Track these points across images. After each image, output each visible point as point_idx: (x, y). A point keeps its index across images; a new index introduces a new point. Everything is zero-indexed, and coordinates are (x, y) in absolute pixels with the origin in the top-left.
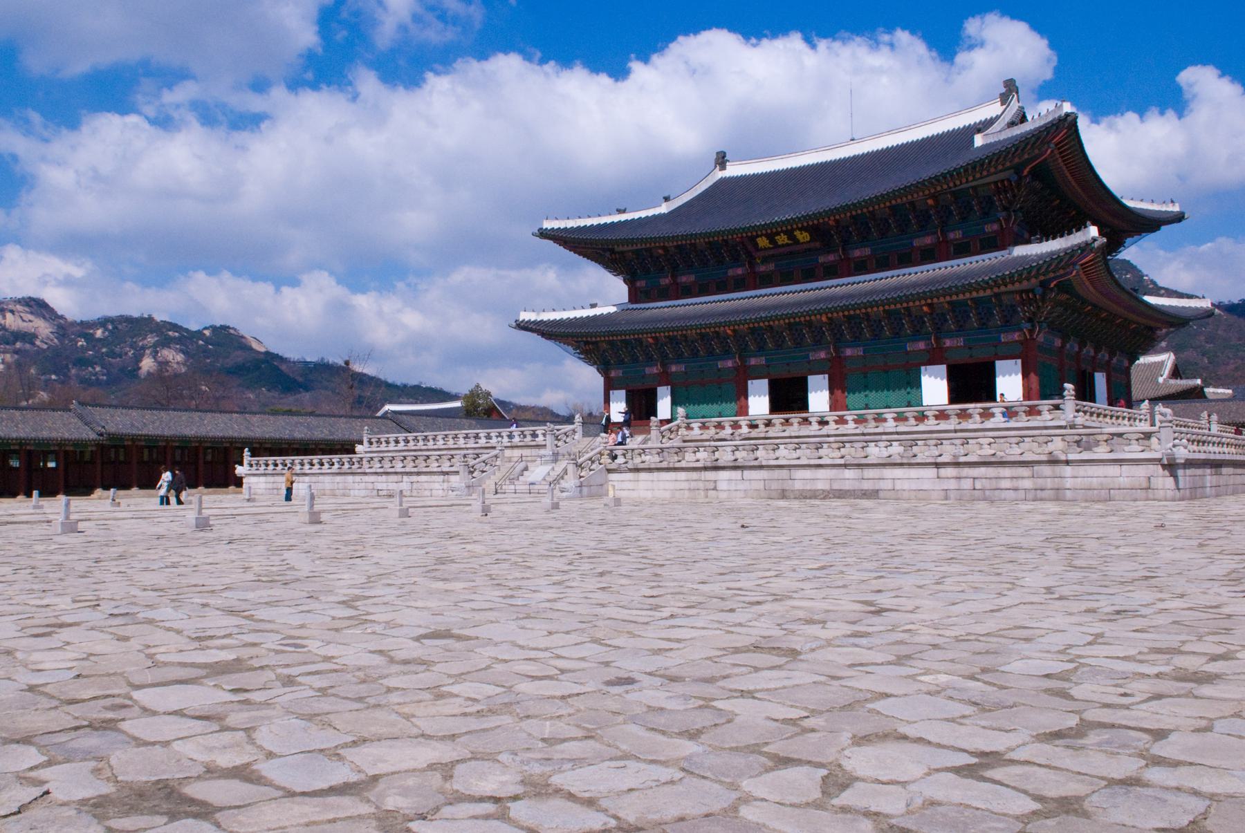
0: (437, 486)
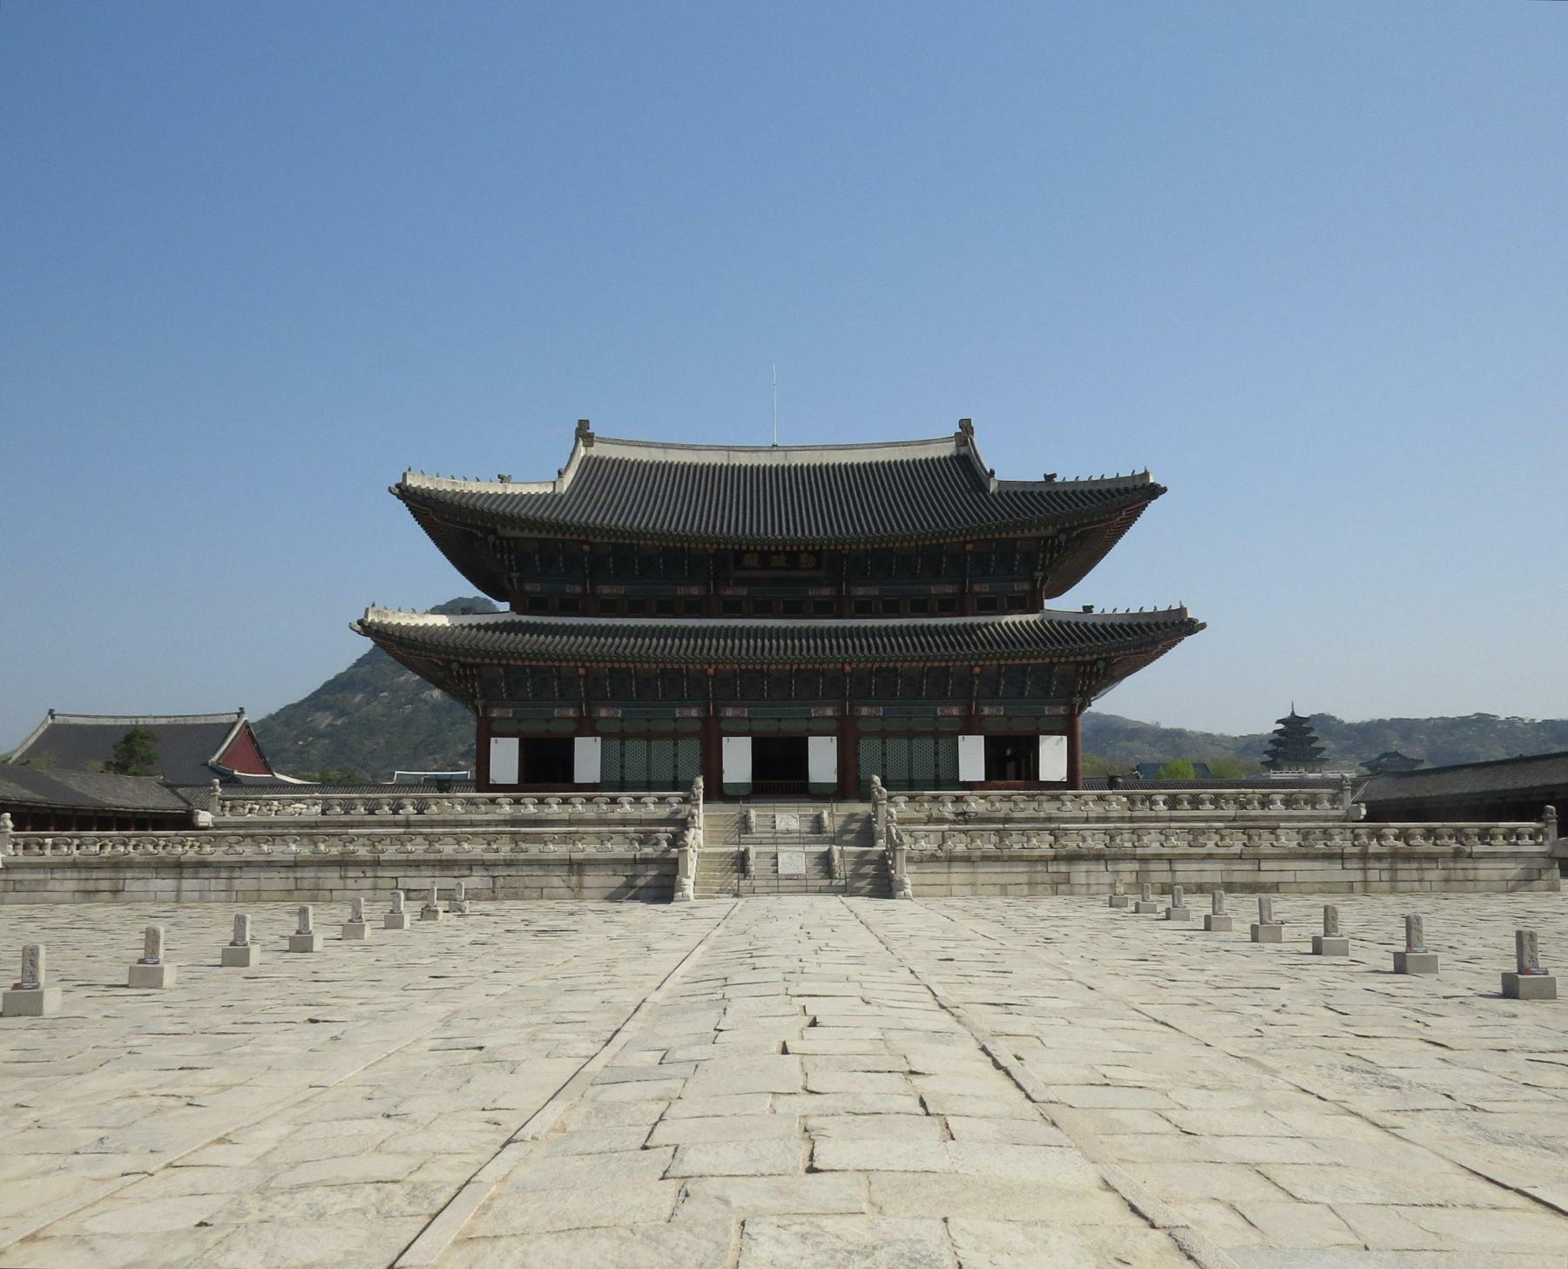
0: (556, 881)
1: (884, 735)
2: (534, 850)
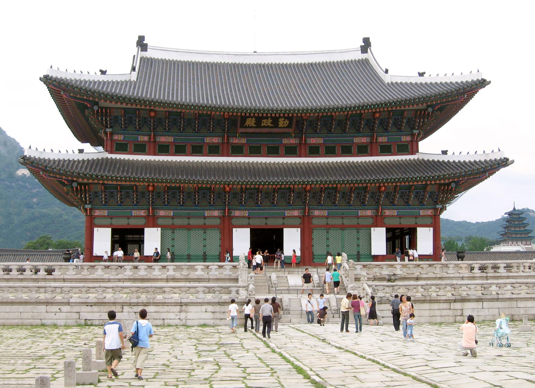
0: (172, 316)
1: (328, 227)
2: (159, 297)
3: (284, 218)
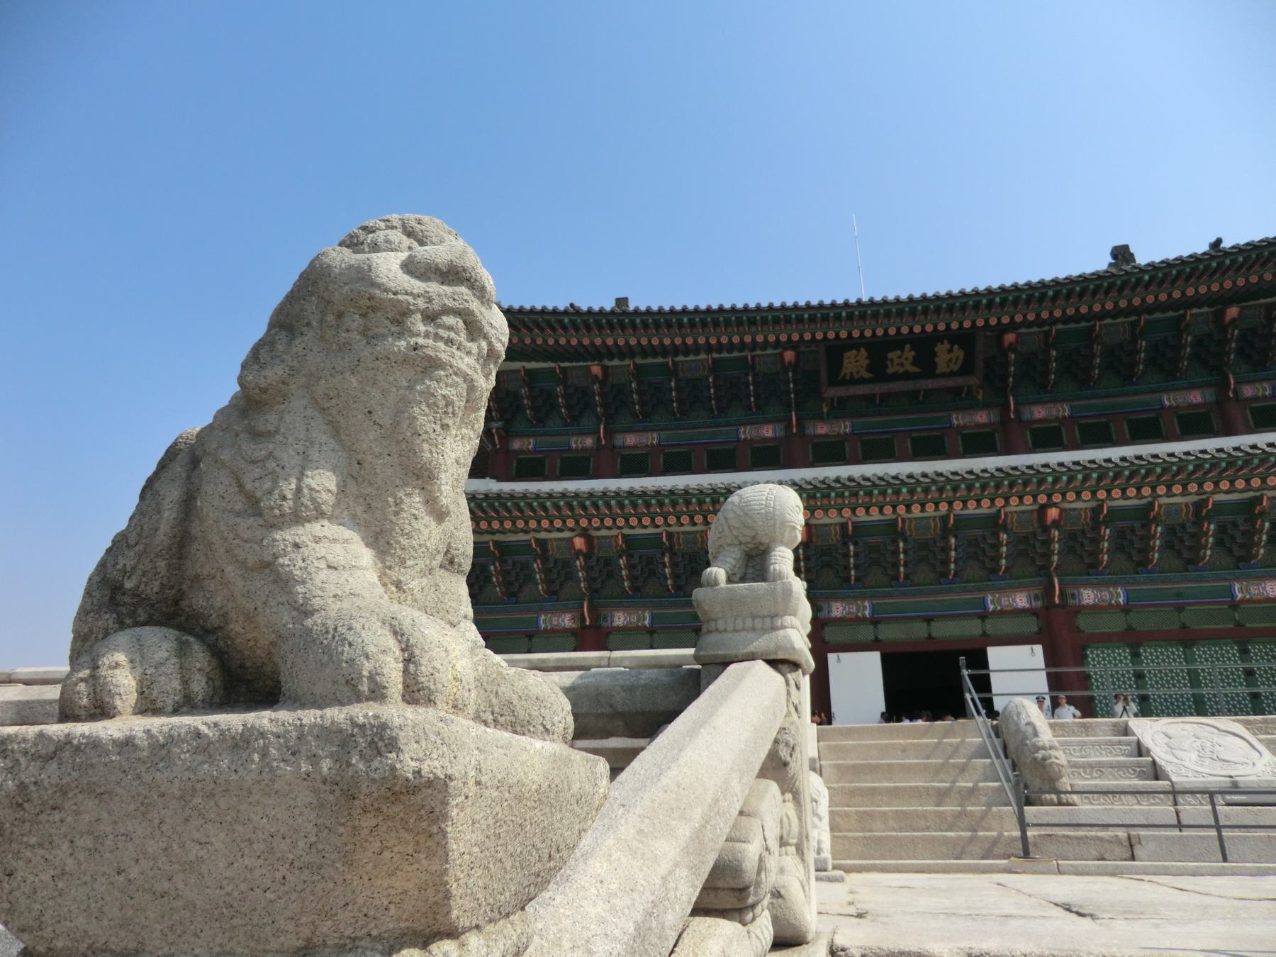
1: (1134, 640)
3: (983, 617)
